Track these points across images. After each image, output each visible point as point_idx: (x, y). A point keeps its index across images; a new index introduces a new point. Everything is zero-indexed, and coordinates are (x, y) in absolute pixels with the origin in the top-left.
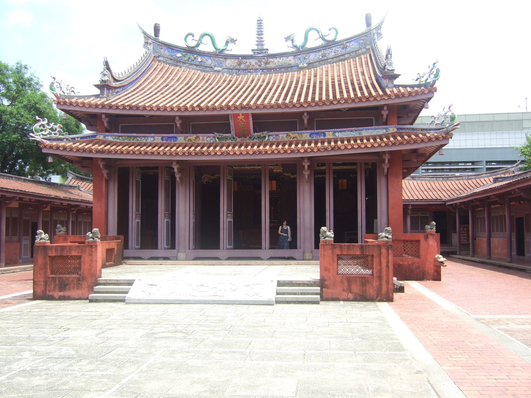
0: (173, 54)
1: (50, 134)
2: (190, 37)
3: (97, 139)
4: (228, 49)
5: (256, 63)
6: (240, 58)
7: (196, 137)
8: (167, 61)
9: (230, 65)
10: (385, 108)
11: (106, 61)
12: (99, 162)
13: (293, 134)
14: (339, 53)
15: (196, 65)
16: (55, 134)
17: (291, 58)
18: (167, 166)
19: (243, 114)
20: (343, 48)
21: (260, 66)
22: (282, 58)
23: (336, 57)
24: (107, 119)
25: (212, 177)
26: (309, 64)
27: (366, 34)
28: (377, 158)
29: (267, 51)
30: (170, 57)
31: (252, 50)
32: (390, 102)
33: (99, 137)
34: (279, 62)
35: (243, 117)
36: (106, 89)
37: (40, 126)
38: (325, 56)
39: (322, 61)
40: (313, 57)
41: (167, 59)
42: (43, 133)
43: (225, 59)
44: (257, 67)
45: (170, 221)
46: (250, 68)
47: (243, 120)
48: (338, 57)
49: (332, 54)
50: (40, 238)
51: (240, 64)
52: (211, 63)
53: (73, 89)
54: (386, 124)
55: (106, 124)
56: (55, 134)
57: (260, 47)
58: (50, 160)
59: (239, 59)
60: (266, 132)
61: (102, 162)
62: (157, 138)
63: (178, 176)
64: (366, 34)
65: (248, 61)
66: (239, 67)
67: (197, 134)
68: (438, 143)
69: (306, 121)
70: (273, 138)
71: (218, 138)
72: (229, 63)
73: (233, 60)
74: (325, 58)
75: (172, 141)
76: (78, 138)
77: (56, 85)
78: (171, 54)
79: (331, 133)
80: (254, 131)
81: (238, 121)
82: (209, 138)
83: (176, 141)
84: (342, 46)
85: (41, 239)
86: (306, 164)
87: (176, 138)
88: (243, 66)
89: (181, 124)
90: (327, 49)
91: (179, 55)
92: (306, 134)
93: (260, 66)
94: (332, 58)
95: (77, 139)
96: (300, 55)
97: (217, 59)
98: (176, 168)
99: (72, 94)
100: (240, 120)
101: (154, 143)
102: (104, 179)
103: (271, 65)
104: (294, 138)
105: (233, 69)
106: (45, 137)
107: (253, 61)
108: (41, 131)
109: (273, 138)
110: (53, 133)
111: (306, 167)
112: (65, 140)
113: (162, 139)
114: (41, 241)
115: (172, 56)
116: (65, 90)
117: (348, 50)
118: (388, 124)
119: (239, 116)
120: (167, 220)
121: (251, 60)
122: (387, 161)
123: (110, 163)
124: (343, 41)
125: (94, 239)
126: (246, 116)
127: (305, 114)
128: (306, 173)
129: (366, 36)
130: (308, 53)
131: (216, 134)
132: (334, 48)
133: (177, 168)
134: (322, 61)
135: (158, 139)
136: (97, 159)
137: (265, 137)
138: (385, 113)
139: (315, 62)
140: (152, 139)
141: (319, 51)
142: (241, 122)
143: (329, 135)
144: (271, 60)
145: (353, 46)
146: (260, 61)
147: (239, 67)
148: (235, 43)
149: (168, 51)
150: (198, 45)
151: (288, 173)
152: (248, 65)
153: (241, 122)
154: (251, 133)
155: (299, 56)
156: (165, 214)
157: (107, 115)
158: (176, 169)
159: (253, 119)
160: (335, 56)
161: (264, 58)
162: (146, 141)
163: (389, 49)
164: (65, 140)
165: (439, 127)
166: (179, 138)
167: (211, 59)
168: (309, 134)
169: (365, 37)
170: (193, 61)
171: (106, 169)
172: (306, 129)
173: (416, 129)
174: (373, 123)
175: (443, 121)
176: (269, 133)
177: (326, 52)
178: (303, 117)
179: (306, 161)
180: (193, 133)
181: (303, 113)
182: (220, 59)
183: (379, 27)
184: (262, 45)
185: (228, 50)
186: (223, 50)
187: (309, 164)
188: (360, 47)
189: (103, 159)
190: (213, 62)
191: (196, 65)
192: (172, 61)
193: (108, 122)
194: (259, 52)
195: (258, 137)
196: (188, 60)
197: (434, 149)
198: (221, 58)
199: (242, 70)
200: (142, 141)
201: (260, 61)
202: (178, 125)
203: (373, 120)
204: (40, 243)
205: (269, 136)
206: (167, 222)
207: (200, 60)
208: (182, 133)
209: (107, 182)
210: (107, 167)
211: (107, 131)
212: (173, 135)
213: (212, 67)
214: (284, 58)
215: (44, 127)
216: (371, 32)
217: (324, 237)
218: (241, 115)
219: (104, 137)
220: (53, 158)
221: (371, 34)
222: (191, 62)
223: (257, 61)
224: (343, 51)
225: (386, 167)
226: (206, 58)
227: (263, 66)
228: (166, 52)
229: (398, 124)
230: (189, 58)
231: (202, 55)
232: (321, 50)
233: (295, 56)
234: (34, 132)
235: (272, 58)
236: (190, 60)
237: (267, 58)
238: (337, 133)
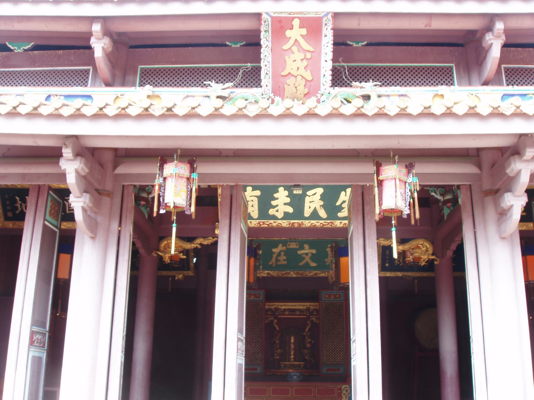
35: (304, 31)
45: (44, 356)
47: (302, 42)
60: (371, 84)
80: (333, 80)
81: (286, 47)
87: (89, 97)
100: (292, 41)
119: (292, 28)
120: (37, 354)
142: (295, 49)
153: (295, 49)
154: (322, 88)
156: (32, 333)
205: (379, 96)
206: (37, 361)
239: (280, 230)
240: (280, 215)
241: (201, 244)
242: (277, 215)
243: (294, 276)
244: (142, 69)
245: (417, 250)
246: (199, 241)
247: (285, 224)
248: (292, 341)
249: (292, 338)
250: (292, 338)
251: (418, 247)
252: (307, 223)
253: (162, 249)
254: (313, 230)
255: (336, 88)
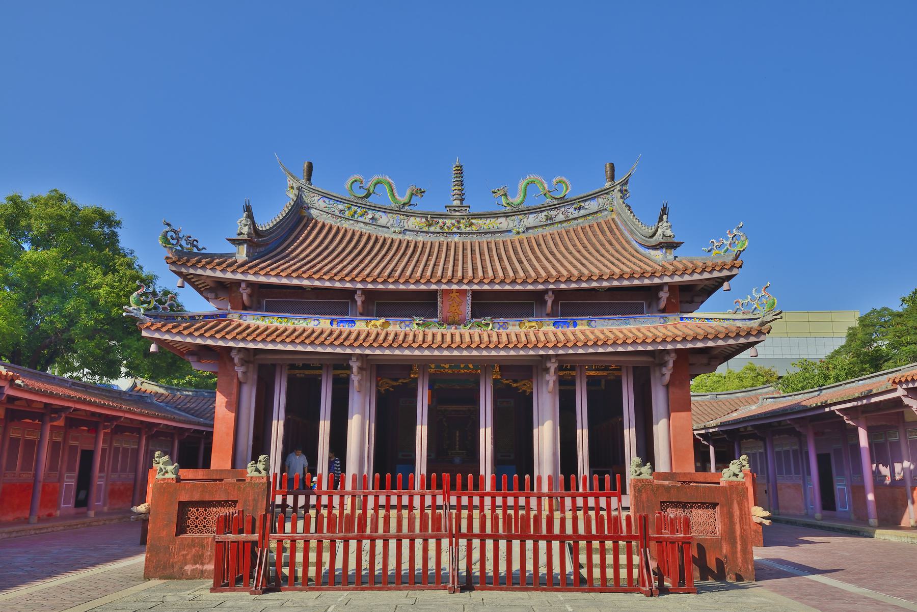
0: (330, 206)
1: (155, 308)
2: (357, 185)
3: (228, 320)
4: (411, 203)
5: (452, 223)
6: (429, 216)
7: (384, 321)
8: (322, 215)
9: (414, 226)
10: (666, 288)
11: (248, 205)
12: (233, 354)
13: (529, 321)
14: (571, 217)
15: (364, 223)
16: (164, 309)
17: (503, 220)
18: (340, 364)
19: (458, 291)
20: (575, 209)
21: (459, 228)
22: (489, 220)
23: (565, 221)
24: (249, 291)
25: (395, 384)
26: (528, 229)
27: (606, 192)
28: (651, 359)
29: (468, 209)
30: (326, 209)
31: (446, 207)
32: (677, 279)
33: (232, 316)
34: (485, 223)
35: (458, 294)
36: (246, 246)
37: (141, 295)
38: (550, 219)
39: (546, 225)
40: (531, 220)
41: (321, 212)
42: (145, 305)
43: (407, 216)
44: (455, 230)
46: (446, 230)
48: (569, 220)
49: (561, 217)
50: (164, 470)
51: (430, 225)
52: (387, 220)
53: (195, 243)
54: (663, 311)
55: (245, 297)
56: (164, 309)
57: (457, 203)
58: (153, 348)
59: (428, 217)
60: (490, 318)
61: (238, 354)
62: (324, 320)
63: (355, 378)
64: (606, 192)
65: (440, 221)
66: (427, 228)
67: (387, 317)
68: (752, 339)
69: (549, 303)
70: (499, 326)
71: (417, 324)
72: (414, 223)
73: (418, 219)
74: (549, 222)
75: (347, 326)
76: (199, 316)
77: (170, 234)
78: (328, 206)
79: (585, 322)
82: (403, 323)
83: (352, 327)
84: (574, 206)
85: (167, 472)
86: (552, 366)
88: (432, 229)
89: (363, 302)
90: (553, 210)
91: (341, 207)
92: (548, 323)
93: (459, 228)
94: (560, 222)
95: (198, 318)
96: (514, 215)
97: (395, 216)
98: (355, 365)
99: (195, 250)
101: (319, 328)
102: (235, 381)
103: (474, 228)
104: (530, 327)
105: (419, 231)
106: (147, 313)
107: (449, 222)
108: (143, 303)
109: (499, 326)
110: (161, 307)
111: (552, 370)
112: (180, 319)
113: (331, 324)
114: (167, 476)
115: (330, 208)
116: (183, 243)
117: (582, 212)
118: (667, 310)
121: (444, 221)
122: (671, 364)
123: (250, 355)
124: (576, 200)
125: (260, 472)
126: (463, 293)
127: (550, 293)
128: (551, 378)
129: (606, 193)
130: (526, 214)
131: (414, 317)
132: (563, 209)
133: (357, 366)
134: (546, 225)
135: (325, 323)
136: (231, 348)
137: (489, 324)
138: (664, 295)
139: (536, 227)
140: (316, 322)
141: (542, 211)
143: (582, 324)
144: (474, 221)
145: (588, 206)
146: (459, 222)
147: (426, 229)
148: (423, 196)
149: (324, 201)
150: (368, 195)
151: (507, 380)
152: (441, 227)
154: (467, 318)
155: (513, 217)
157: (250, 284)
158: (356, 368)
159: (472, 300)
160: (564, 219)
161: (463, 219)
162: (307, 325)
163: (665, 206)
164: (180, 319)
165: (750, 316)
166: (357, 323)
167: (387, 217)
168: (553, 322)
169: (606, 195)
170: (361, 216)
171: (242, 365)
172: (548, 315)
173: (712, 319)
174: (643, 310)
175: (756, 308)
176: (493, 319)
177: (553, 213)
178: (546, 297)
179: (553, 360)
180: (379, 315)
181: (546, 291)
182: (399, 215)
183: (626, 182)
184: (462, 200)
185: (410, 205)
186: (404, 205)
187: (556, 365)
188: (600, 207)
189: (240, 350)
190: (391, 219)
191: (364, 223)
192: (330, 215)
193: (250, 296)
194: (456, 209)
195: (478, 325)
196: (353, 216)
197: (727, 352)
198: (401, 215)
199: (431, 233)
200: (301, 325)
201: (459, 222)
202: (359, 303)
203: (643, 305)
204: (165, 479)
205: (494, 323)
207: (370, 216)
208: (362, 314)
209: (240, 384)
210: (244, 362)
211: (245, 308)
212: (348, 317)
213: (388, 228)
214: (493, 220)
215: (147, 297)
216: (613, 189)
217: (638, 473)
218: (454, 291)
219: (241, 317)
220: (159, 348)
221: (613, 190)
222: (357, 218)
223: (454, 221)
224: (576, 214)
225: (667, 372)
226: (380, 213)
227: (464, 229)
228: (321, 202)
229: (682, 312)
230: (355, 212)
231: (372, 210)
232: (544, 211)
233: (509, 216)
234: (132, 304)
235: (475, 218)
236: (356, 216)
237: (468, 218)
238: (594, 322)
239: (447, 373)
240: (447, 366)
241: (402, 382)
242: (445, 366)
243: (458, 388)
244: (377, 303)
245: (524, 386)
246: (400, 381)
247: (450, 371)
248: (457, 434)
249: (458, 432)
250: (458, 432)
251: (524, 385)
252: (462, 371)
253: (380, 385)
254: (465, 374)
255: (474, 319)
